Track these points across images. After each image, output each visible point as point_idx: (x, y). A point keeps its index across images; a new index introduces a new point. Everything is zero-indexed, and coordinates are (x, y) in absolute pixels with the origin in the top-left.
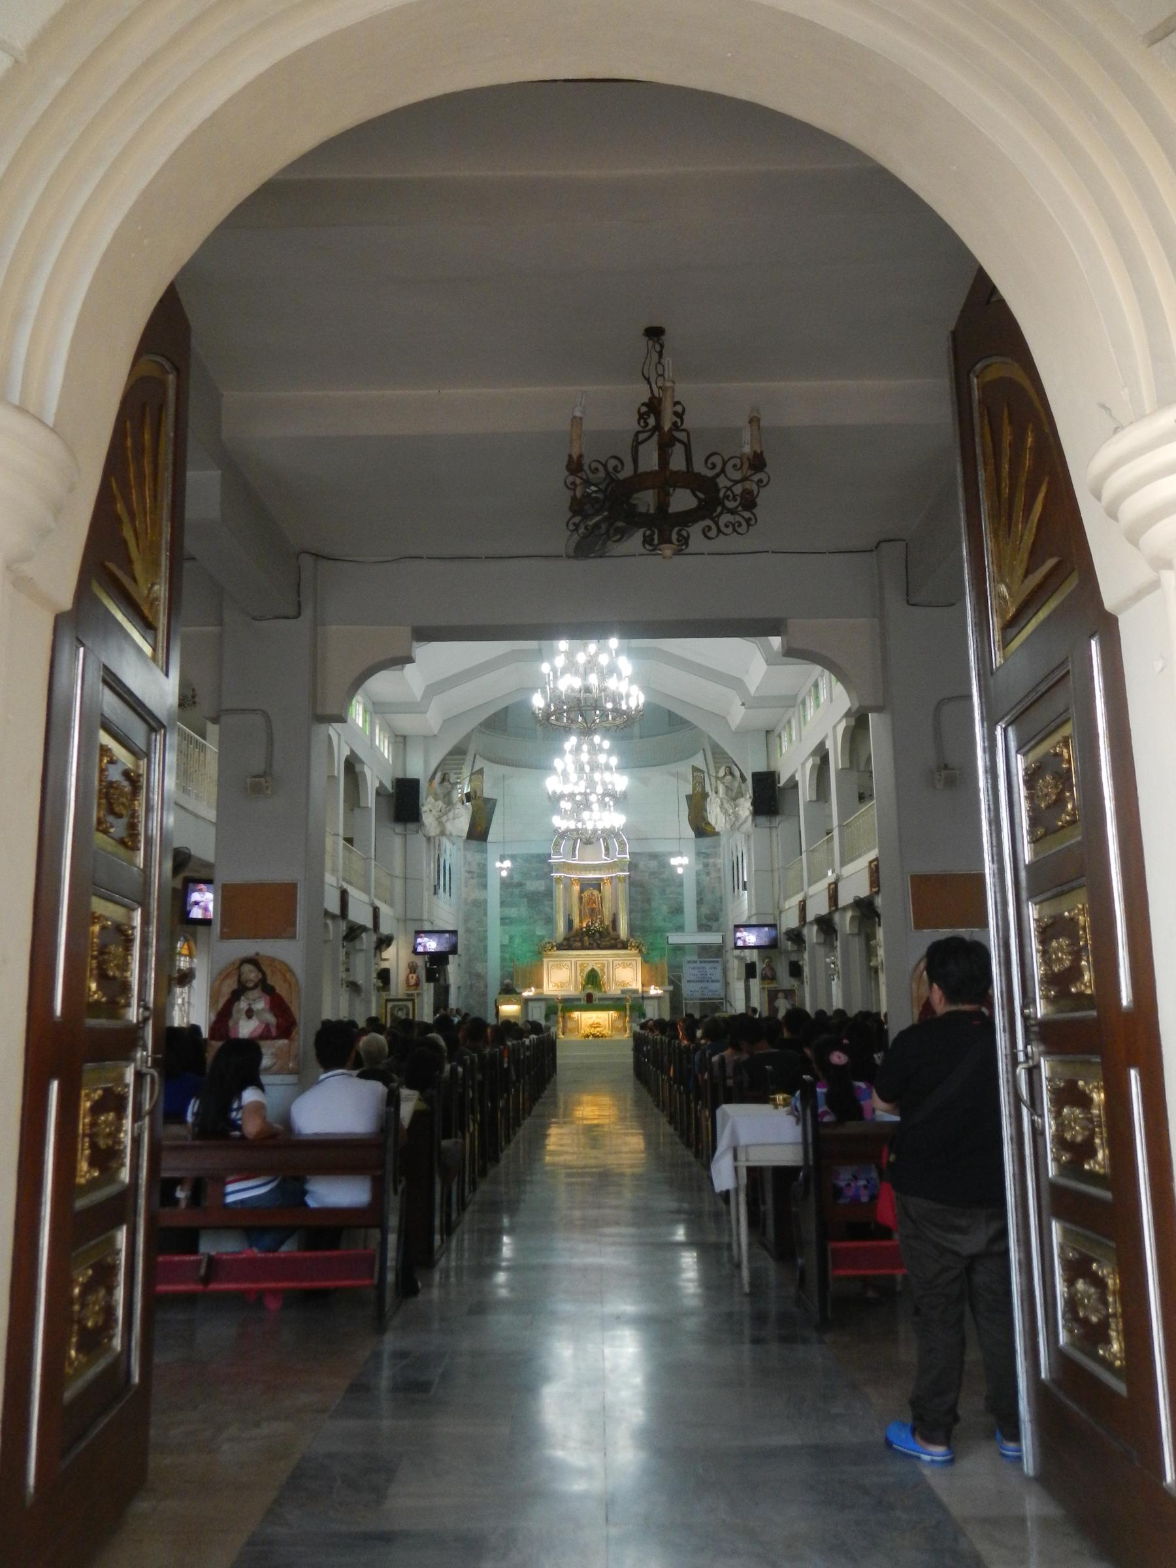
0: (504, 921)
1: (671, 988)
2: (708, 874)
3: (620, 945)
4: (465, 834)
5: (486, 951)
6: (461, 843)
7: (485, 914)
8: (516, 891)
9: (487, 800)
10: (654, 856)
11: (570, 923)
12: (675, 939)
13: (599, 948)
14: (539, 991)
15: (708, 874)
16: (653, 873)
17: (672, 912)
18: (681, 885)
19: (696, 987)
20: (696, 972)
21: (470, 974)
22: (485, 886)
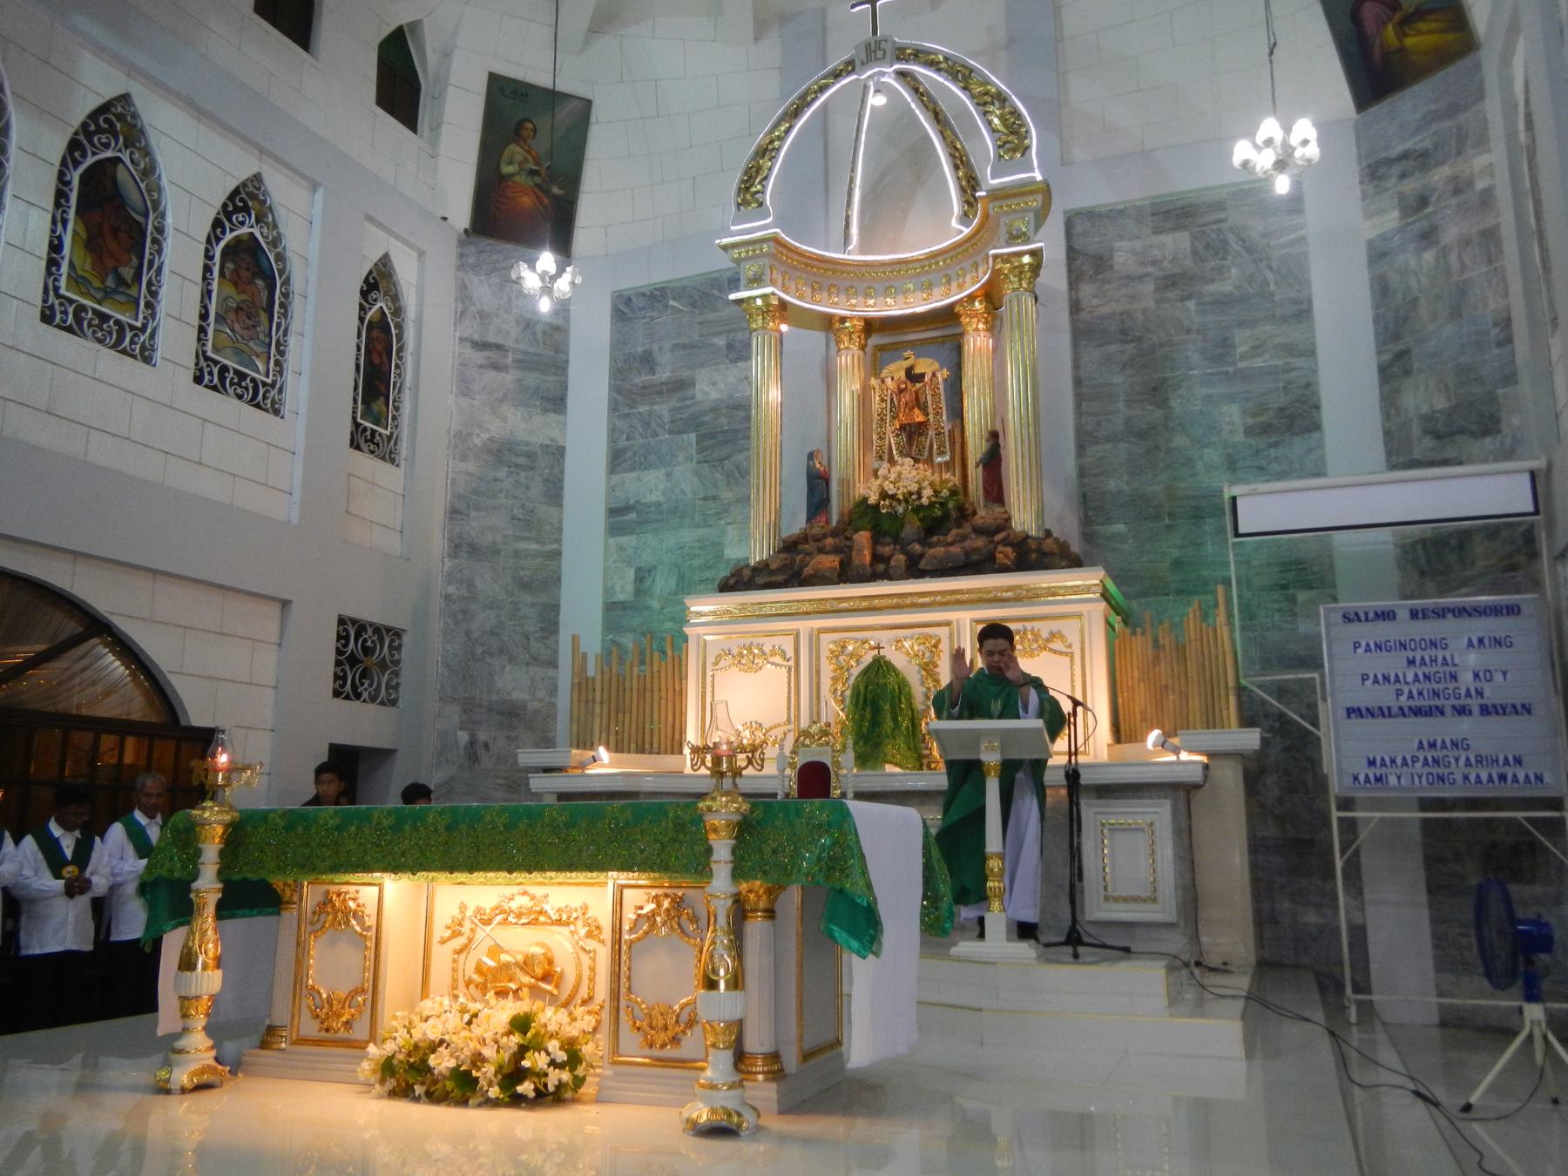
0: (622, 518)
1: (1250, 739)
2: (1428, 237)
3: (1005, 554)
4: (461, 212)
5: (550, 626)
6: (452, 249)
7: (554, 493)
8: (663, 409)
9: (553, 98)
10: (1174, 214)
11: (818, 485)
12: (1265, 508)
13: (915, 571)
14: (668, 762)
15: (1428, 237)
16: (1171, 282)
17: (1265, 429)
18: (1303, 312)
19: (1399, 738)
20: (1393, 663)
21: (469, 707)
22: (557, 402)
